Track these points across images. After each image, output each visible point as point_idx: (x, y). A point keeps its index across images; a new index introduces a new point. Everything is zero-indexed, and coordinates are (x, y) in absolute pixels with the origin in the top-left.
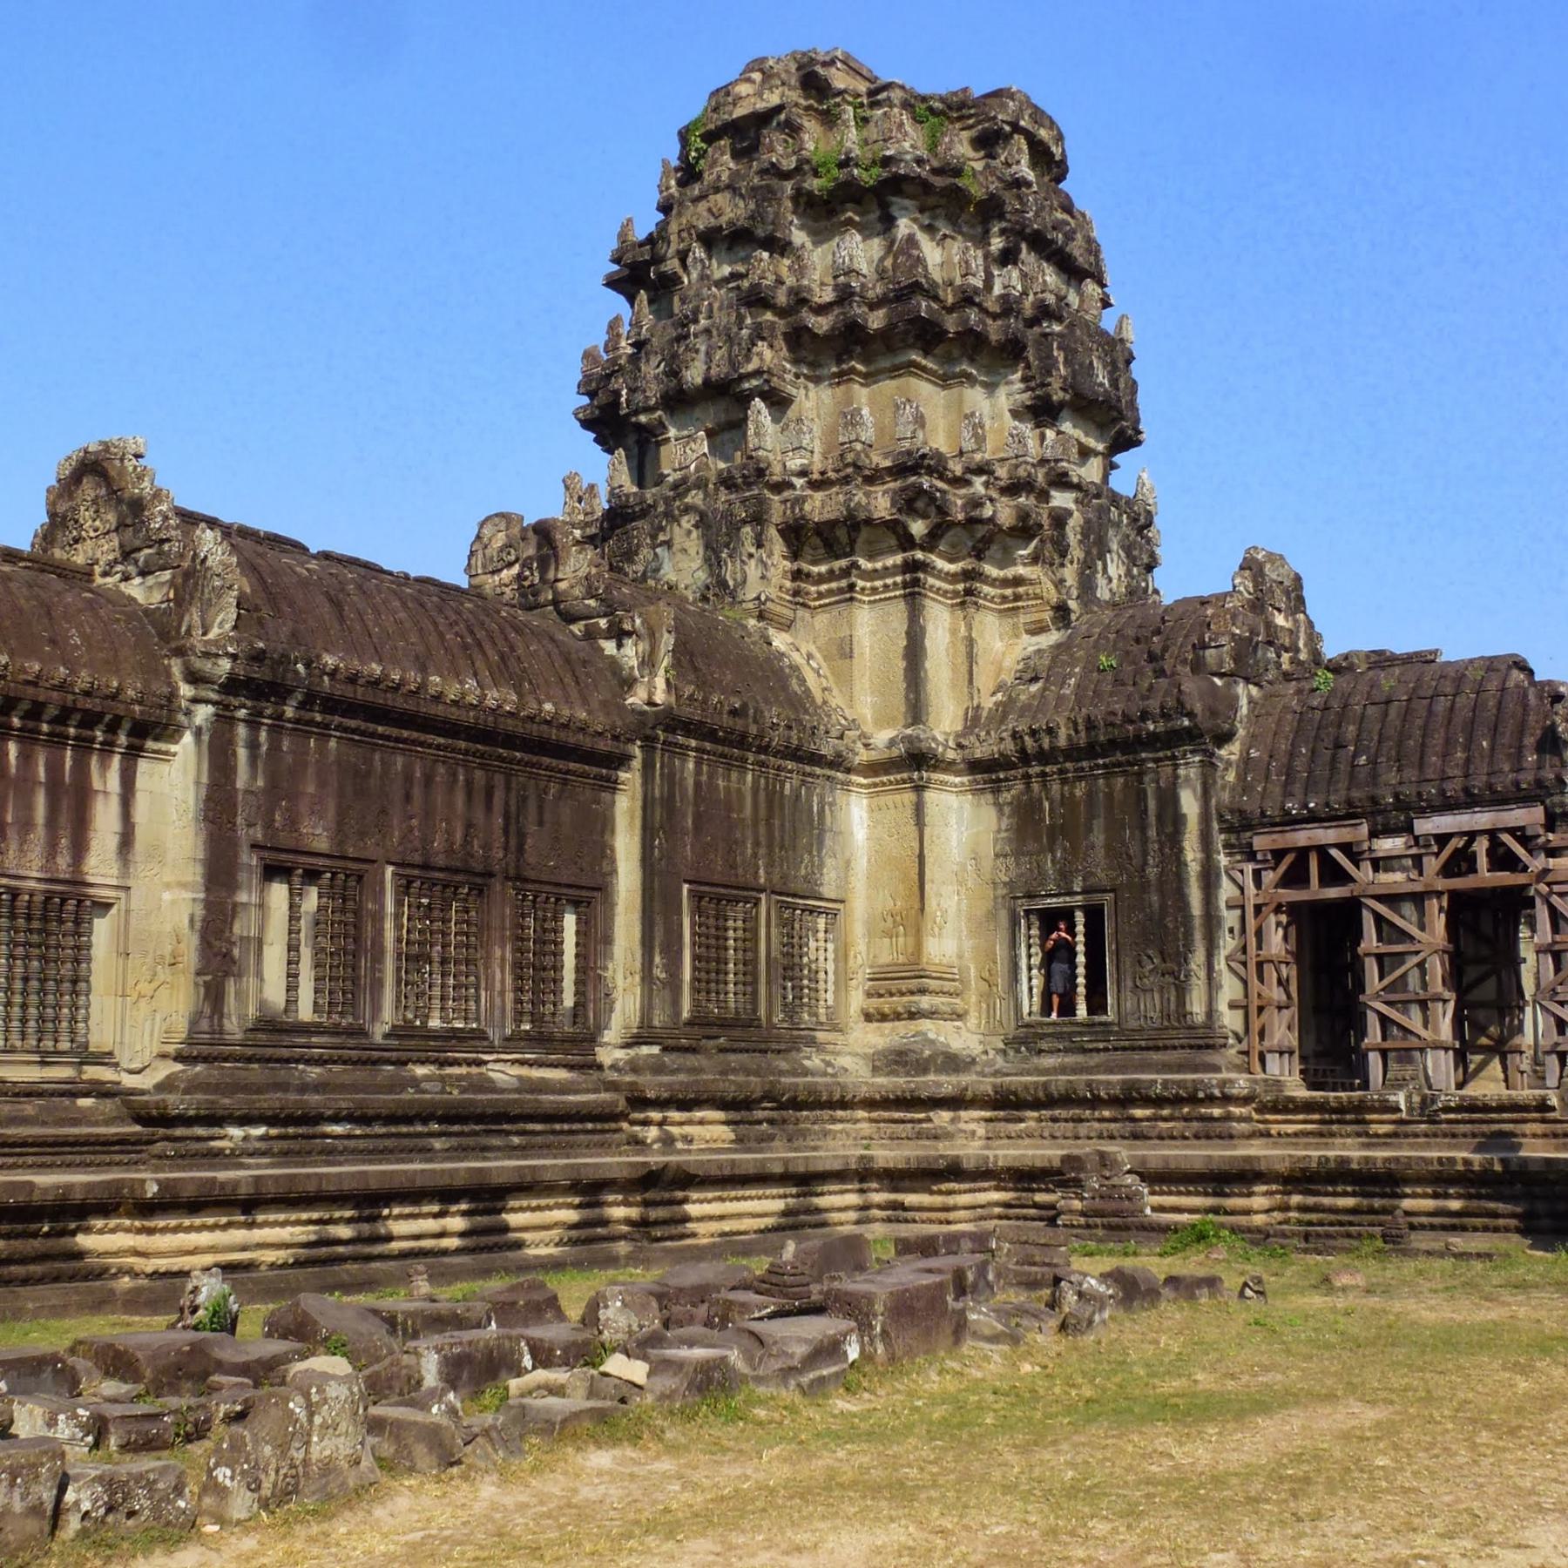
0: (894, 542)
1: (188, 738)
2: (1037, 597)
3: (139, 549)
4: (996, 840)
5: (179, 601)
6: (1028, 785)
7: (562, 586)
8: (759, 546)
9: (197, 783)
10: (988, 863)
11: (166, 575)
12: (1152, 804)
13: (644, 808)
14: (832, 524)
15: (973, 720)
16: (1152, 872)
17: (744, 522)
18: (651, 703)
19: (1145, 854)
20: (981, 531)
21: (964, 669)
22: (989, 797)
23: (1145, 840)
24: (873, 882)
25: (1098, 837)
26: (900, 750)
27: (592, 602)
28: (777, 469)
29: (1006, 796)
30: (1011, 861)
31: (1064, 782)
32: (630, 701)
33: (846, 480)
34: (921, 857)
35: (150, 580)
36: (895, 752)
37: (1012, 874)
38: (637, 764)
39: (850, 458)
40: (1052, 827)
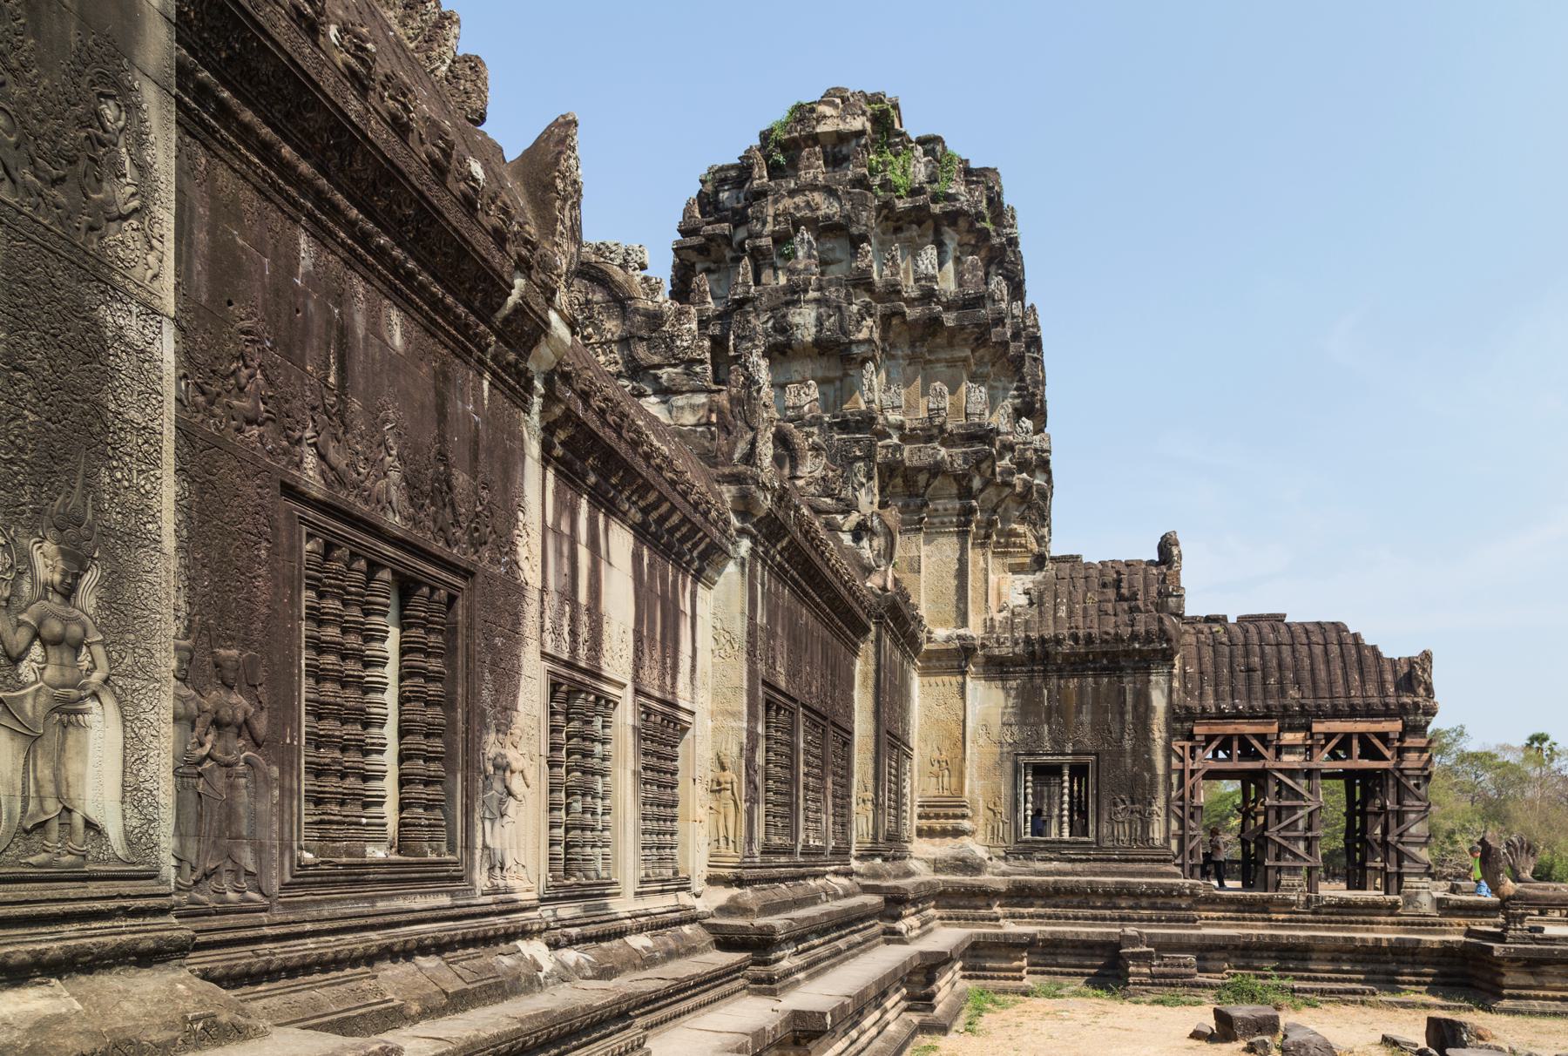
0: (954, 491)
1: (731, 568)
2: (1021, 546)
3: (659, 367)
4: (1003, 714)
5: (724, 426)
6: (1031, 678)
7: (800, 483)
8: (870, 478)
9: (743, 613)
10: (996, 730)
11: (701, 399)
12: (1129, 698)
13: (877, 671)
14: (919, 470)
15: (990, 627)
16: (1128, 744)
17: (858, 459)
18: (884, 589)
19: (1123, 731)
20: (1007, 491)
21: (982, 591)
22: (999, 683)
23: (1123, 722)
24: (924, 740)
25: (1086, 718)
26: (956, 644)
27: (828, 500)
28: (881, 420)
29: (1013, 684)
30: (1015, 729)
31: (1060, 677)
32: (869, 584)
33: (929, 439)
34: (964, 721)
35: (679, 401)
36: (952, 646)
37: (1017, 738)
38: (872, 636)
39: (937, 421)
40: (1049, 708)
